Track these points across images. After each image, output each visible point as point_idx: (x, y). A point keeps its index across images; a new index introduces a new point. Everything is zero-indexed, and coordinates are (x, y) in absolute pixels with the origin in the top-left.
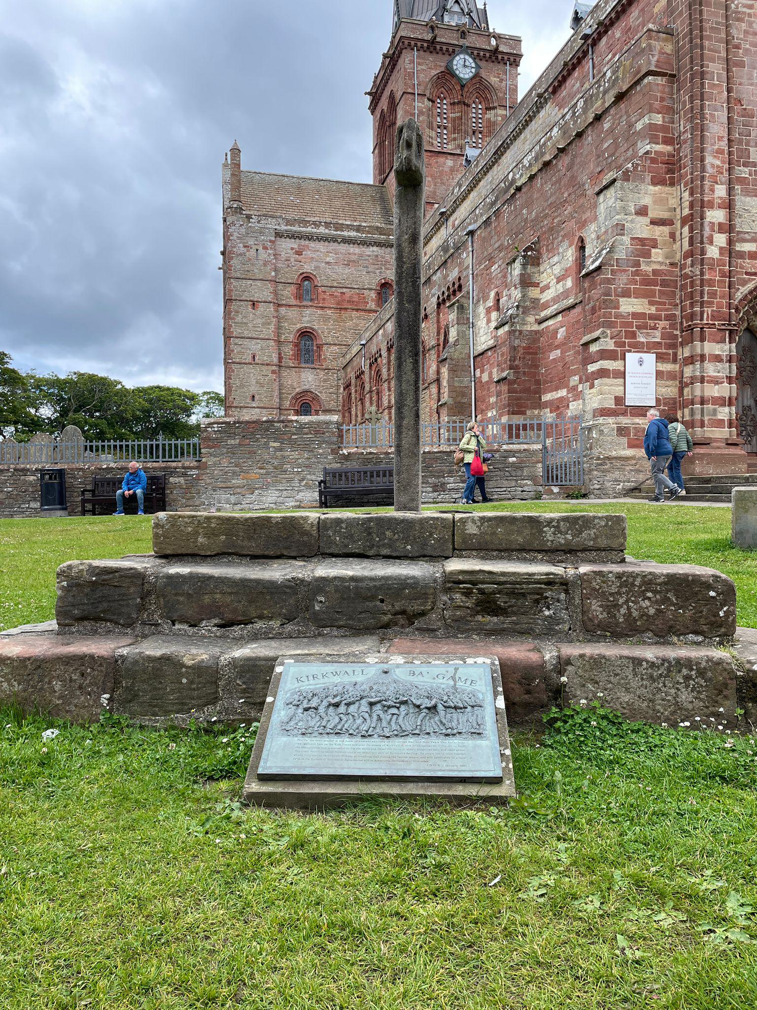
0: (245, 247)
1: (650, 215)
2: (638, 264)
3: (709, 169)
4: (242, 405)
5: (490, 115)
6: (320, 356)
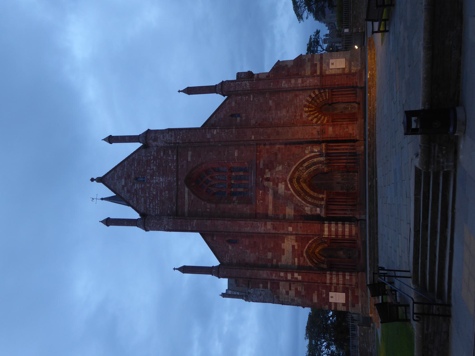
0: (261, 296)
1: (288, 290)
2: (303, 296)
3: (276, 278)
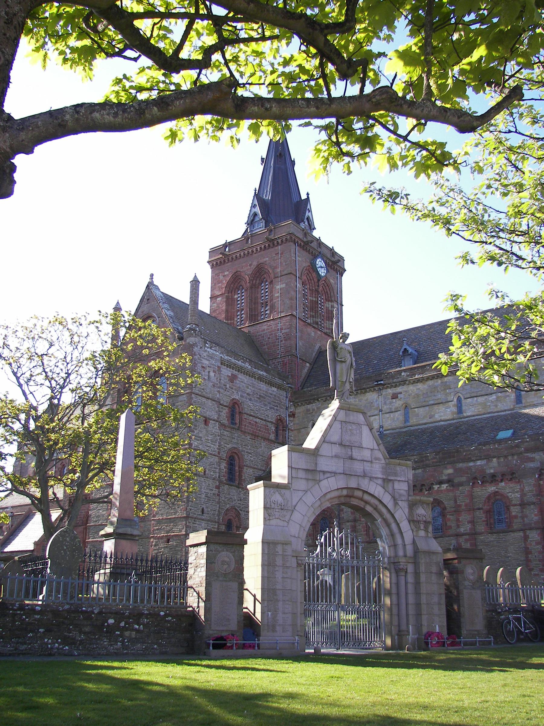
4: (195, 516)
5: (328, 305)
6: (240, 476)
